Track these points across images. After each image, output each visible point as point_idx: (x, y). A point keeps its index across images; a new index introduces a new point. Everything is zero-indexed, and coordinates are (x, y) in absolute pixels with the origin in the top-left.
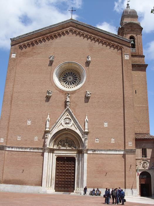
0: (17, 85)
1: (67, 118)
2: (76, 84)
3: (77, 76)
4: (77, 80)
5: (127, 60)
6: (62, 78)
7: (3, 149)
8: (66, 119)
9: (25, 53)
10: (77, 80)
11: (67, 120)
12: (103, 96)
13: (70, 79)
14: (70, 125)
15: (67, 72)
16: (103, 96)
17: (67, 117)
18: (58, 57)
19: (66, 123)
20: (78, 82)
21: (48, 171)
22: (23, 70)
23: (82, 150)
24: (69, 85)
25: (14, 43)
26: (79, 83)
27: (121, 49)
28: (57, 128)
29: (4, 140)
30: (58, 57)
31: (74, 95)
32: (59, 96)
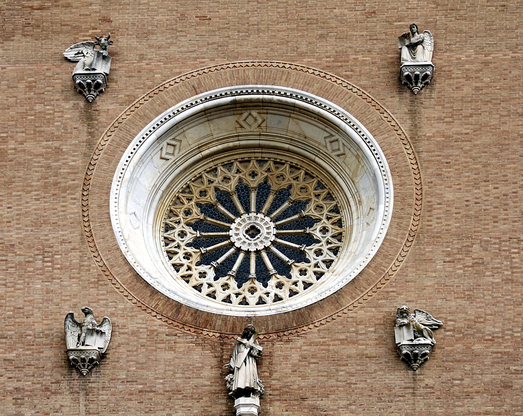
2: (303, 272)
3: (310, 211)
4: (310, 240)
10: (310, 240)
15: (226, 179)
20: (319, 253)
31: (300, 342)
32: (169, 355)
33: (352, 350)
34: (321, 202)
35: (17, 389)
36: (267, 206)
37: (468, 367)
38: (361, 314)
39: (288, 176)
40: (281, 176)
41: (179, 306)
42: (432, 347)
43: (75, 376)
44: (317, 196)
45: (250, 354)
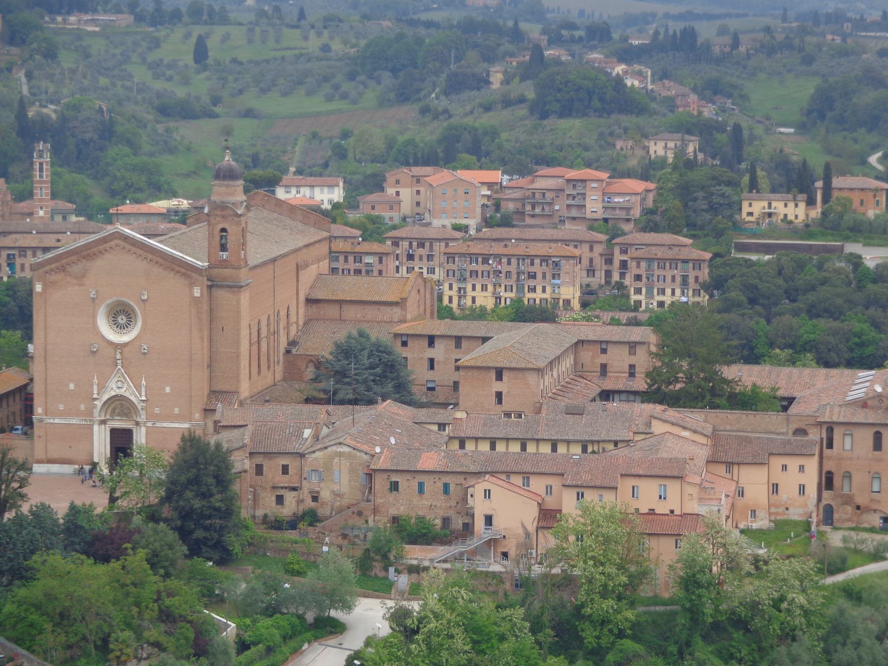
9: (54, 283)
14: (123, 390)
17: (120, 379)
19: (119, 388)
27: (189, 277)
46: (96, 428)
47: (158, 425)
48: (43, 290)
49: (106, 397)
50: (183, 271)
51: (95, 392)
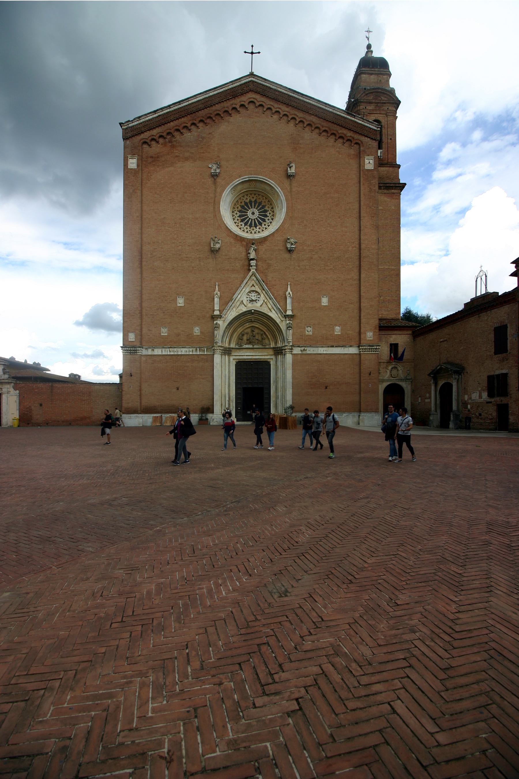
0: (148, 228)
1: (253, 291)
3: (266, 208)
4: (266, 216)
5: (368, 170)
6: (236, 214)
7: (136, 353)
8: (250, 292)
10: (266, 216)
11: (253, 295)
12: (320, 247)
13: (253, 213)
14: (259, 304)
15: (247, 199)
16: (320, 247)
17: (253, 289)
18: (227, 167)
19: (252, 301)
20: (268, 220)
21: (223, 387)
22: (156, 196)
23: (279, 348)
24: (252, 228)
25: (129, 135)
26: (271, 222)
28: (234, 309)
29: (136, 337)
30: (227, 167)
31: (265, 246)
32: (235, 249)
33: (277, 248)
34: (269, 206)
35: (199, 257)
36: (256, 206)
37: (303, 253)
38: (279, 238)
39: (261, 199)
40: (260, 198)
41: (237, 235)
42: (295, 248)
43: (213, 254)
44: (268, 204)
45: (254, 249)
46: (217, 358)
47: (310, 350)
48: (138, 166)
49: (231, 314)
50: (349, 134)
51: (217, 307)
